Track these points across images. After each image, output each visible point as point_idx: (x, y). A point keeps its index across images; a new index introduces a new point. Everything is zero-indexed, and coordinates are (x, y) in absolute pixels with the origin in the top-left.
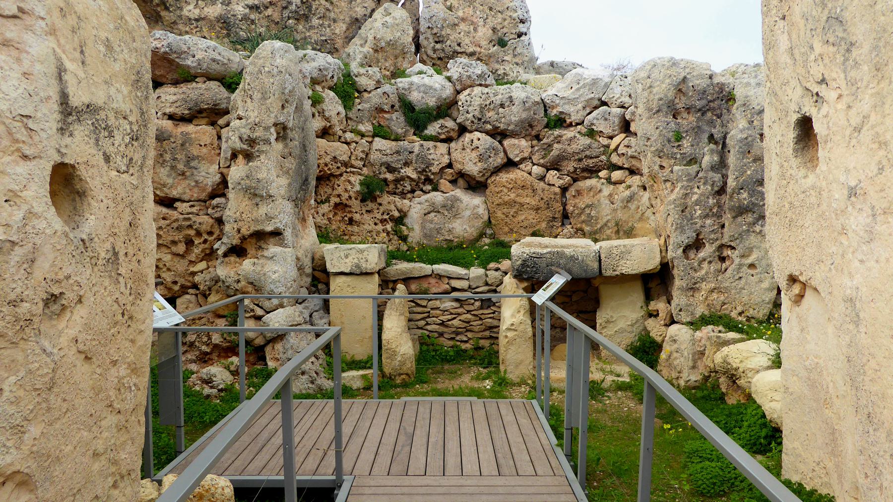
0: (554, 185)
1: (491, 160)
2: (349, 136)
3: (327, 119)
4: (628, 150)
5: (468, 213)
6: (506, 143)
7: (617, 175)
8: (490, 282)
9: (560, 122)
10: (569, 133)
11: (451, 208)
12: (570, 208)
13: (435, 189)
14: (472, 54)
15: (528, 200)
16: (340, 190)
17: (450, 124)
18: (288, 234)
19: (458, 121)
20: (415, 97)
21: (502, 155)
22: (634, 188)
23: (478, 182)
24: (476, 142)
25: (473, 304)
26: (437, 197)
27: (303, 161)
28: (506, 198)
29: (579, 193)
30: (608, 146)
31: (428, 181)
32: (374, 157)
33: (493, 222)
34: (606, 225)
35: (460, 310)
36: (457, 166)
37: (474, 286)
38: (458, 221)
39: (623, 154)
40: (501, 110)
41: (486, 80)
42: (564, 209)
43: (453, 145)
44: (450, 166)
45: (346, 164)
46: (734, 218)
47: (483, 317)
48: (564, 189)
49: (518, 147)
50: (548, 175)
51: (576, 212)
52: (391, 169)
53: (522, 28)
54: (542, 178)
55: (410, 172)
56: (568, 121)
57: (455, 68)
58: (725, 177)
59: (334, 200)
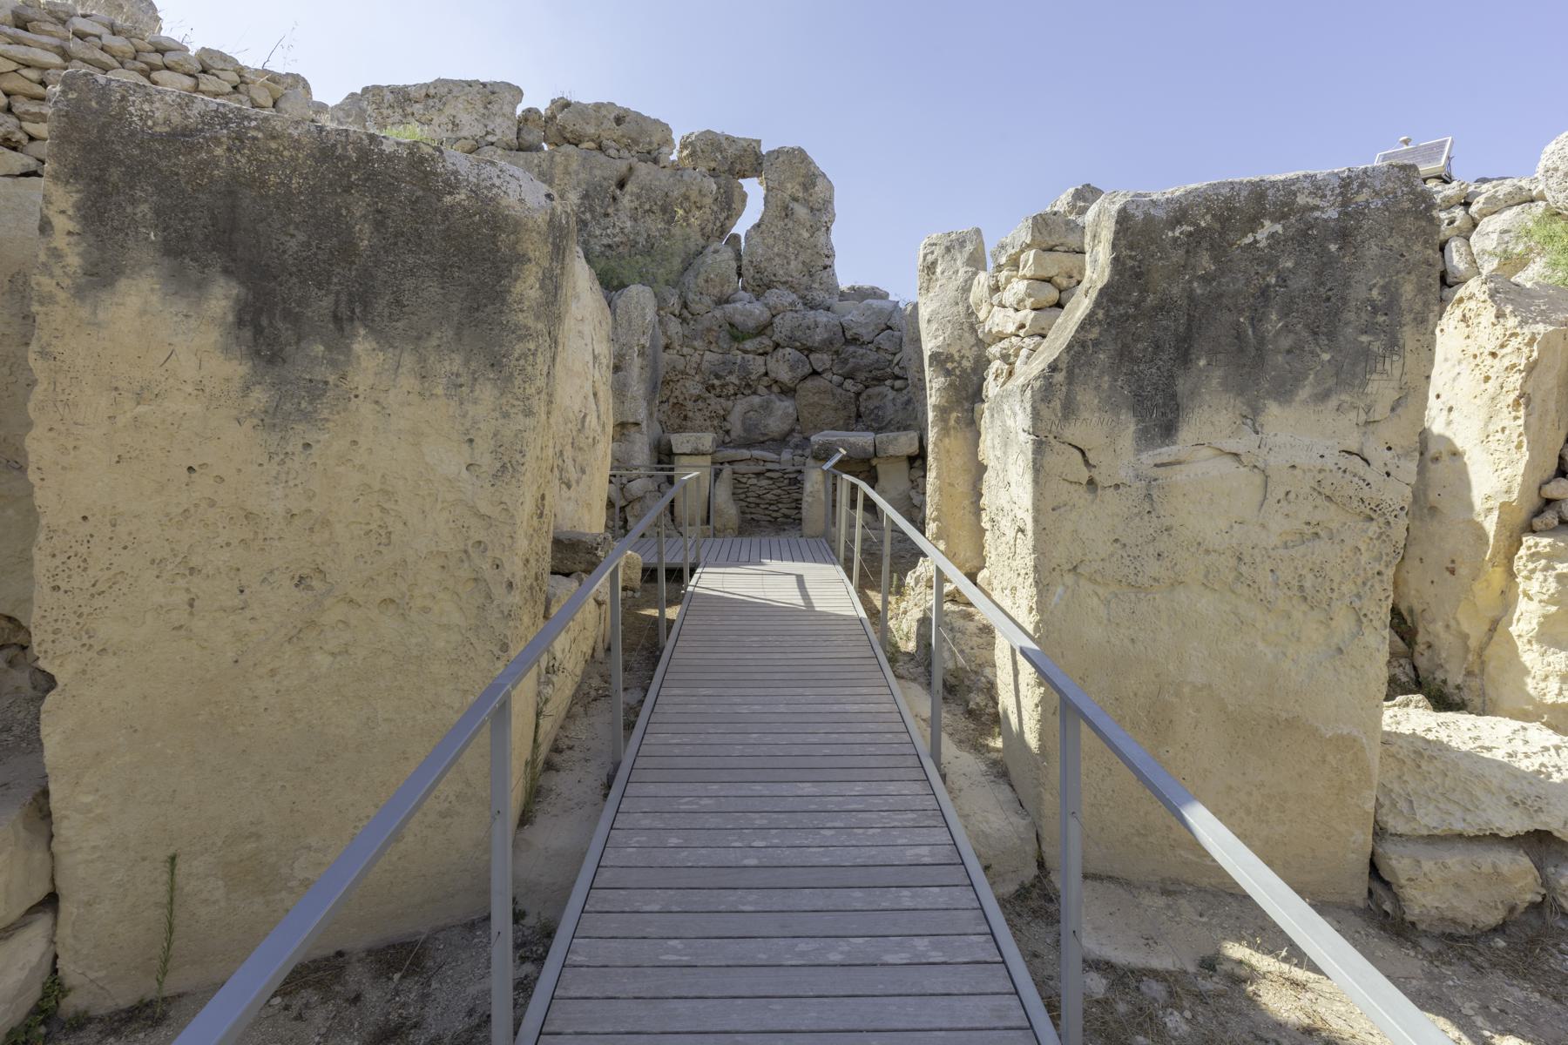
2: (685, 350)
3: (669, 338)
9: (854, 340)
10: (861, 351)
11: (766, 407)
12: (862, 409)
13: (755, 393)
14: (785, 283)
16: (677, 393)
17: (766, 341)
18: (644, 425)
20: (738, 319)
26: (756, 400)
27: (655, 369)
29: (869, 397)
31: (747, 387)
32: (705, 365)
36: (772, 375)
44: (766, 374)
45: (682, 373)
48: (858, 394)
49: (821, 360)
52: (718, 377)
53: (828, 262)
54: (840, 385)
55: (733, 379)
57: (773, 297)
59: (672, 400)
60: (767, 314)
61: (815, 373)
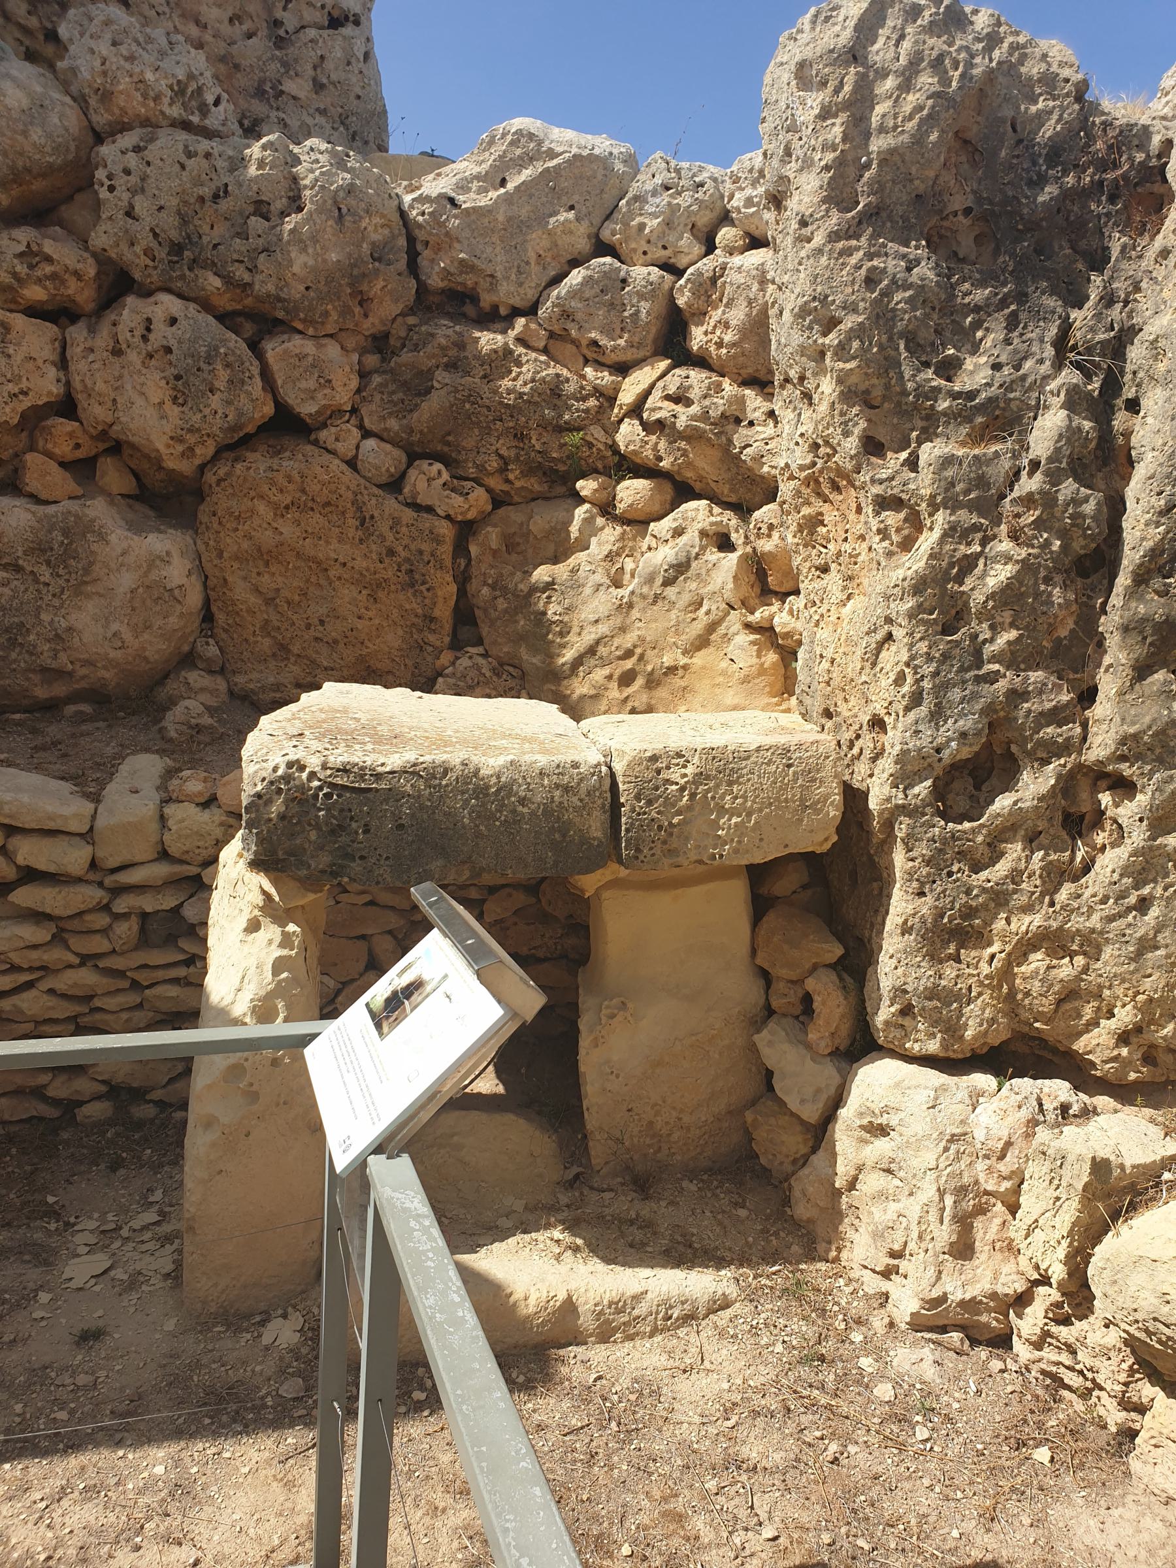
0: (430, 509)
1: (215, 401)
4: (679, 408)
5: (126, 581)
6: (273, 349)
7: (632, 492)
8: (173, 850)
11: (63, 556)
15: (342, 551)
17: (61, 251)
19: (100, 238)
21: (256, 386)
22: (691, 537)
23: (173, 476)
24: (161, 334)
25: (105, 931)
28: (267, 538)
30: (609, 398)
33: (220, 618)
34: (592, 651)
35: (55, 955)
37: (113, 863)
38: (91, 606)
39: (660, 423)
40: (256, 223)
41: (204, 110)
42: (462, 592)
43: (77, 333)
44: (67, 407)
46: (1141, 671)
47: (143, 977)
50: (412, 474)
51: (501, 604)
54: (394, 485)
56: (486, 300)
58: (1116, 506)
60: (63, 119)
61: (287, 426)
